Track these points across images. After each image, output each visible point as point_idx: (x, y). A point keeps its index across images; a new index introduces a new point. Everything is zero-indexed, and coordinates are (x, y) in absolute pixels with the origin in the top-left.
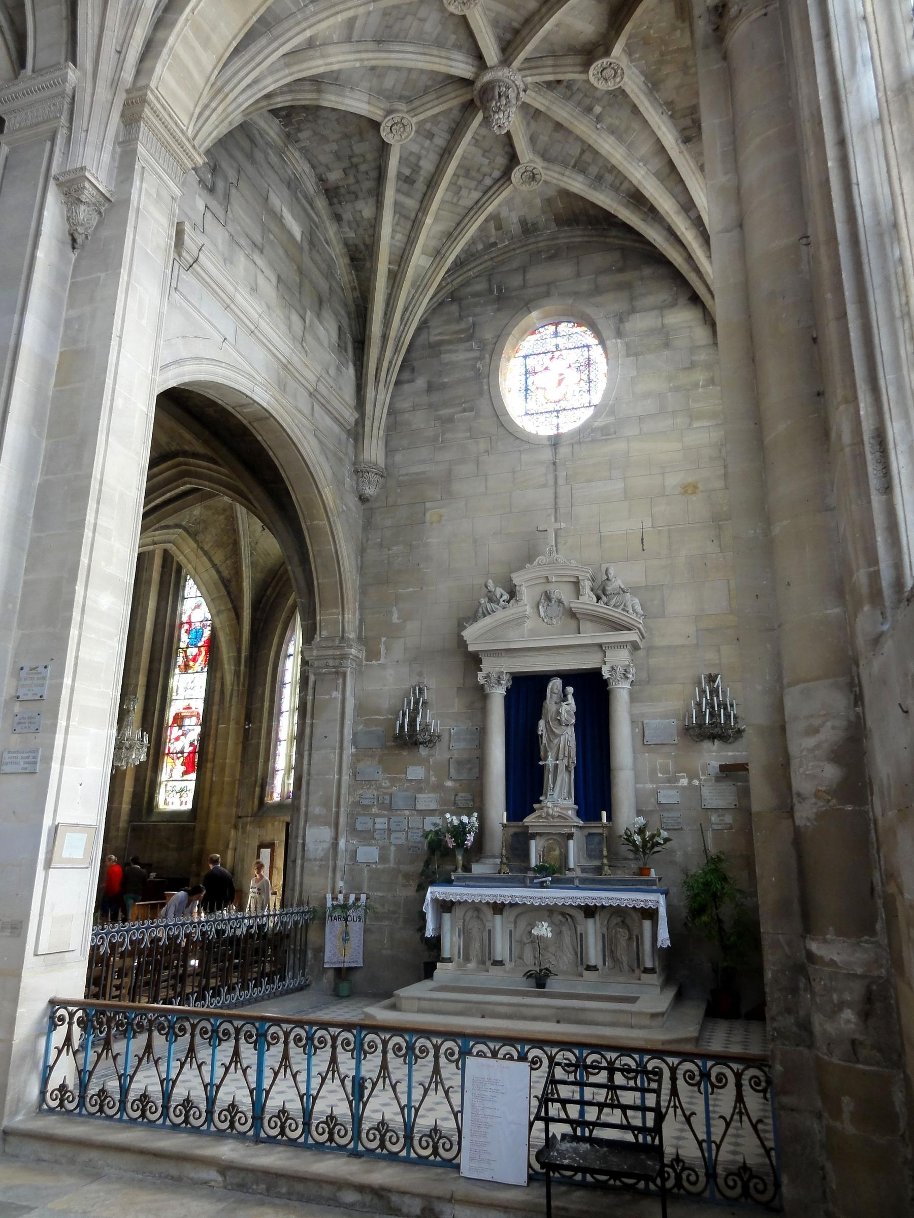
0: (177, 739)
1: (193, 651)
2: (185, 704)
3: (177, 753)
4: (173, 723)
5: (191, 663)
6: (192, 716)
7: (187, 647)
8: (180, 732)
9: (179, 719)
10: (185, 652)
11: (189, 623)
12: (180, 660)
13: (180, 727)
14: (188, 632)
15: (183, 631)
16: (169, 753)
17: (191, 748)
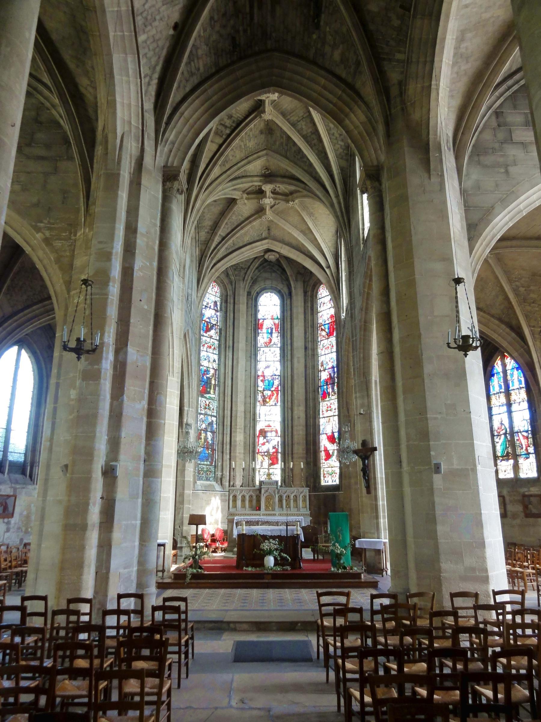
0: (264, 444)
1: (269, 393)
2: (267, 423)
3: (264, 453)
4: (259, 434)
5: (268, 400)
6: (272, 431)
7: (264, 390)
8: (265, 440)
9: (263, 433)
10: (263, 393)
11: (264, 376)
12: (259, 398)
13: (265, 437)
14: (262, 381)
15: (259, 381)
16: (258, 453)
17: (274, 450)
